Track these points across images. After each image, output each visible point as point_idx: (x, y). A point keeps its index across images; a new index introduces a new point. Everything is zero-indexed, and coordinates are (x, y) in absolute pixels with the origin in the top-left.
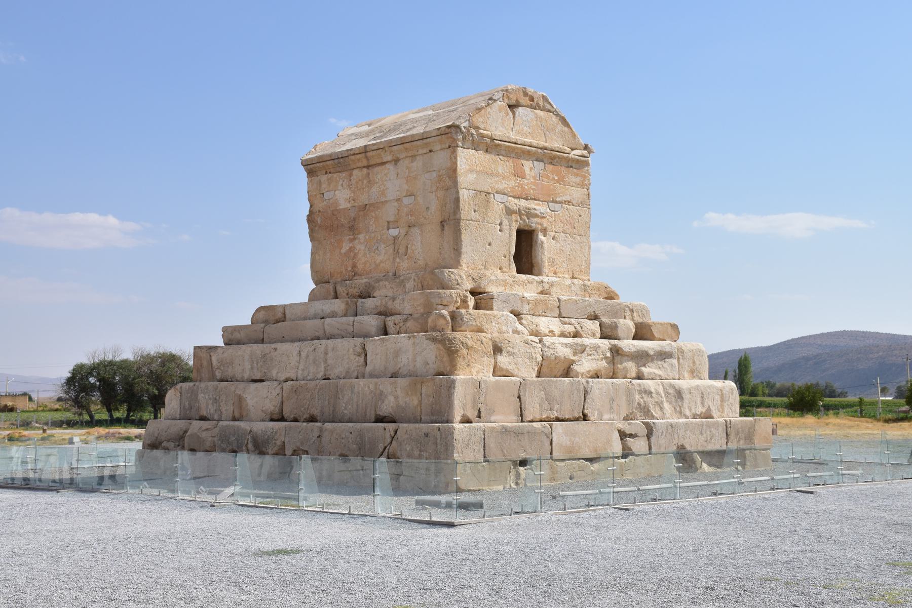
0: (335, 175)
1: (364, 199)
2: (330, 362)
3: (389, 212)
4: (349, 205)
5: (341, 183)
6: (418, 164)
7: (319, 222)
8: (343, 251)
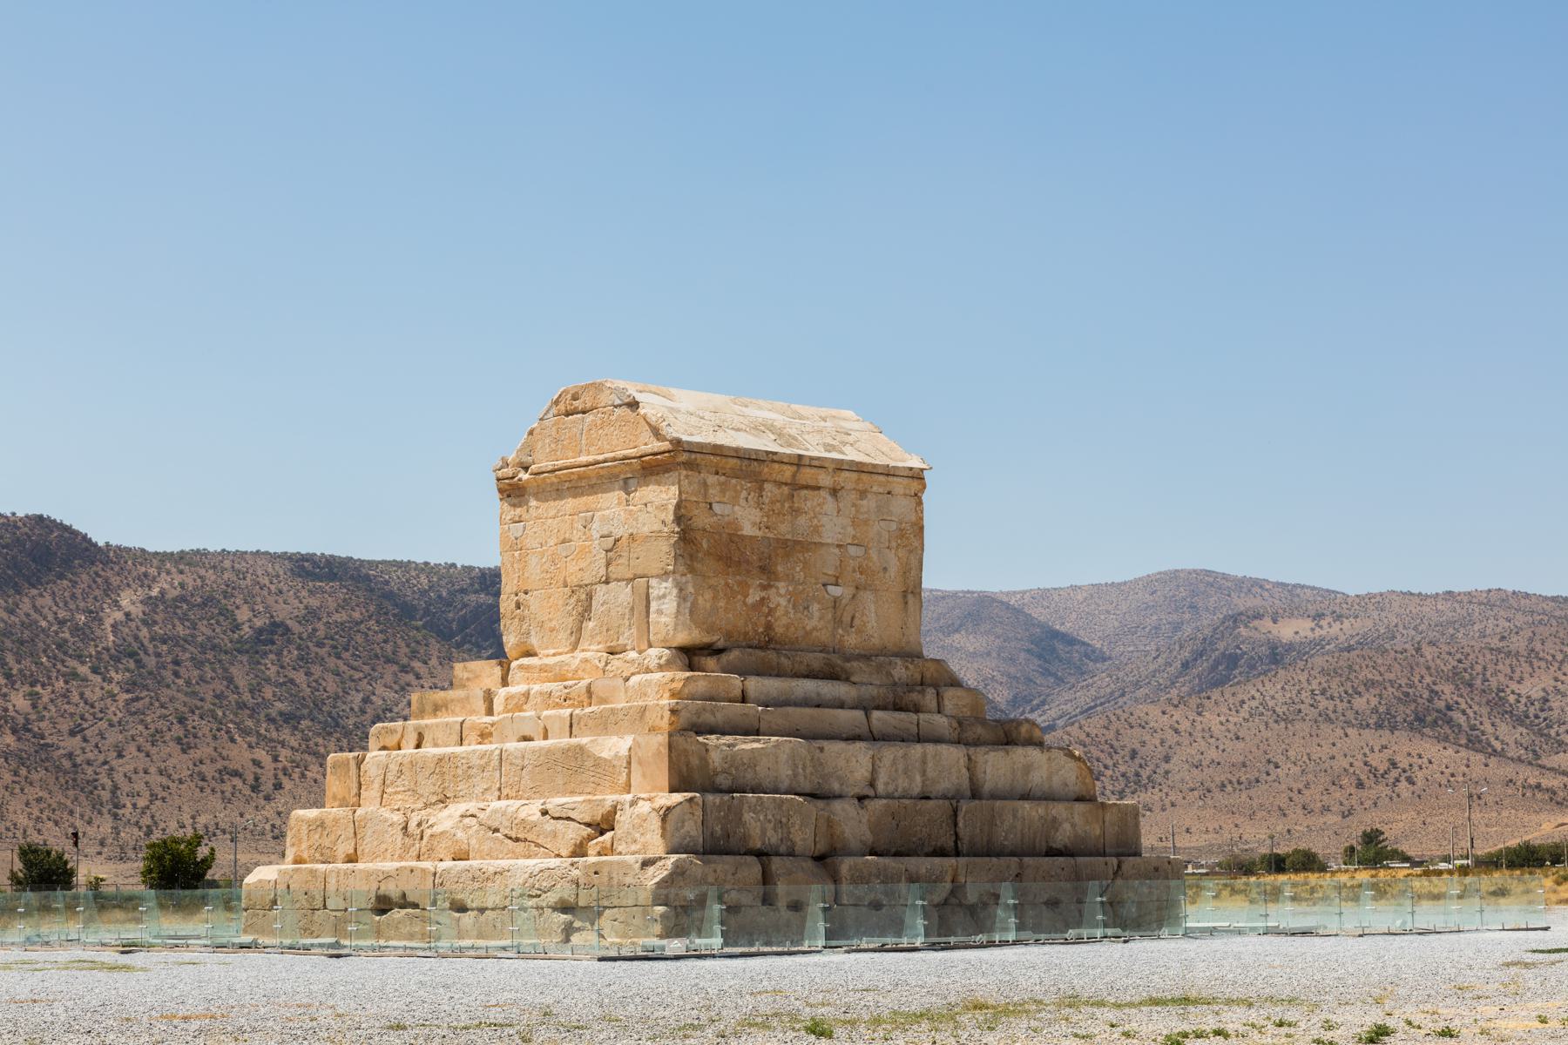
0: (734, 481)
1: (784, 529)
2: (931, 773)
3: (828, 561)
4: (759, 534)
5: (744, 494)
6: (869, 504)
7: (705, 546)
8: (750, 600)
